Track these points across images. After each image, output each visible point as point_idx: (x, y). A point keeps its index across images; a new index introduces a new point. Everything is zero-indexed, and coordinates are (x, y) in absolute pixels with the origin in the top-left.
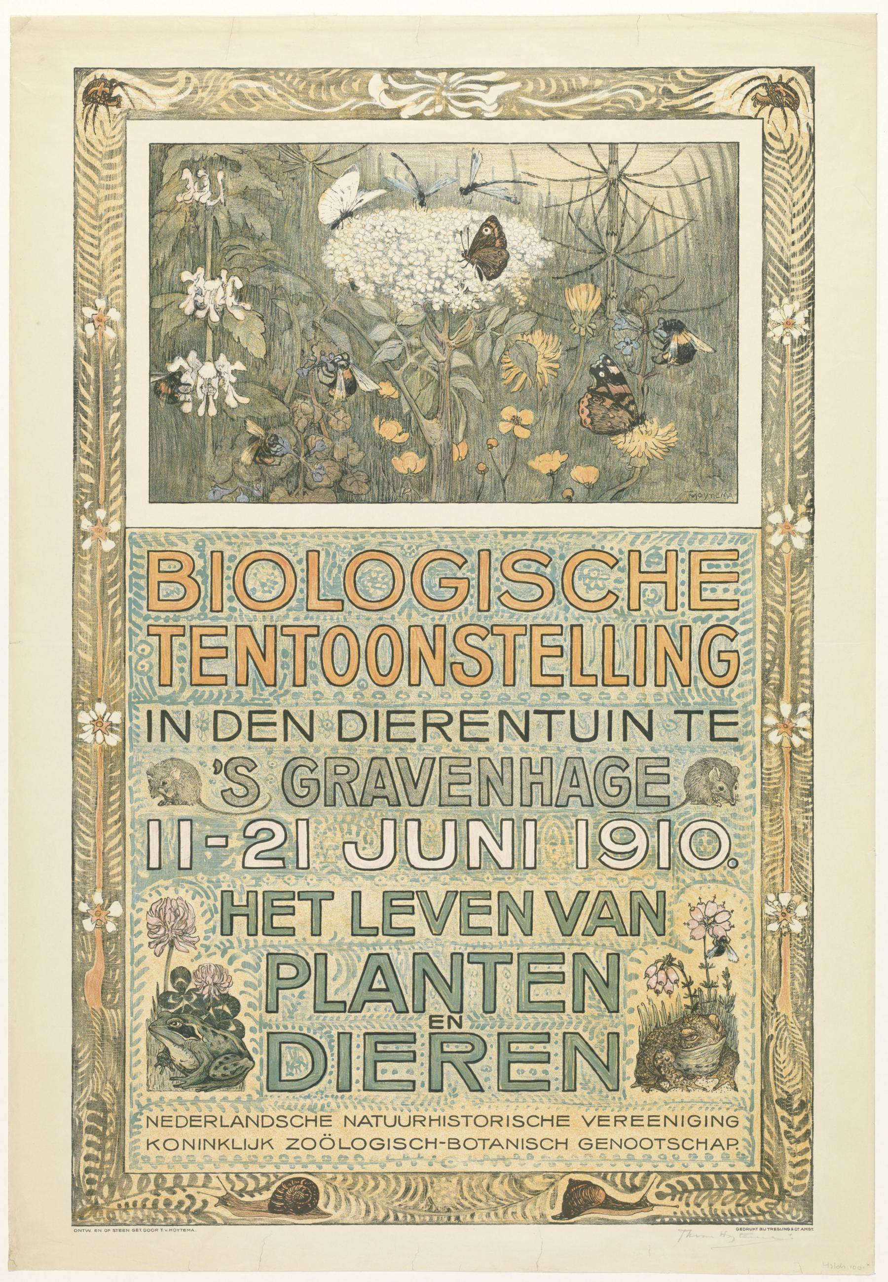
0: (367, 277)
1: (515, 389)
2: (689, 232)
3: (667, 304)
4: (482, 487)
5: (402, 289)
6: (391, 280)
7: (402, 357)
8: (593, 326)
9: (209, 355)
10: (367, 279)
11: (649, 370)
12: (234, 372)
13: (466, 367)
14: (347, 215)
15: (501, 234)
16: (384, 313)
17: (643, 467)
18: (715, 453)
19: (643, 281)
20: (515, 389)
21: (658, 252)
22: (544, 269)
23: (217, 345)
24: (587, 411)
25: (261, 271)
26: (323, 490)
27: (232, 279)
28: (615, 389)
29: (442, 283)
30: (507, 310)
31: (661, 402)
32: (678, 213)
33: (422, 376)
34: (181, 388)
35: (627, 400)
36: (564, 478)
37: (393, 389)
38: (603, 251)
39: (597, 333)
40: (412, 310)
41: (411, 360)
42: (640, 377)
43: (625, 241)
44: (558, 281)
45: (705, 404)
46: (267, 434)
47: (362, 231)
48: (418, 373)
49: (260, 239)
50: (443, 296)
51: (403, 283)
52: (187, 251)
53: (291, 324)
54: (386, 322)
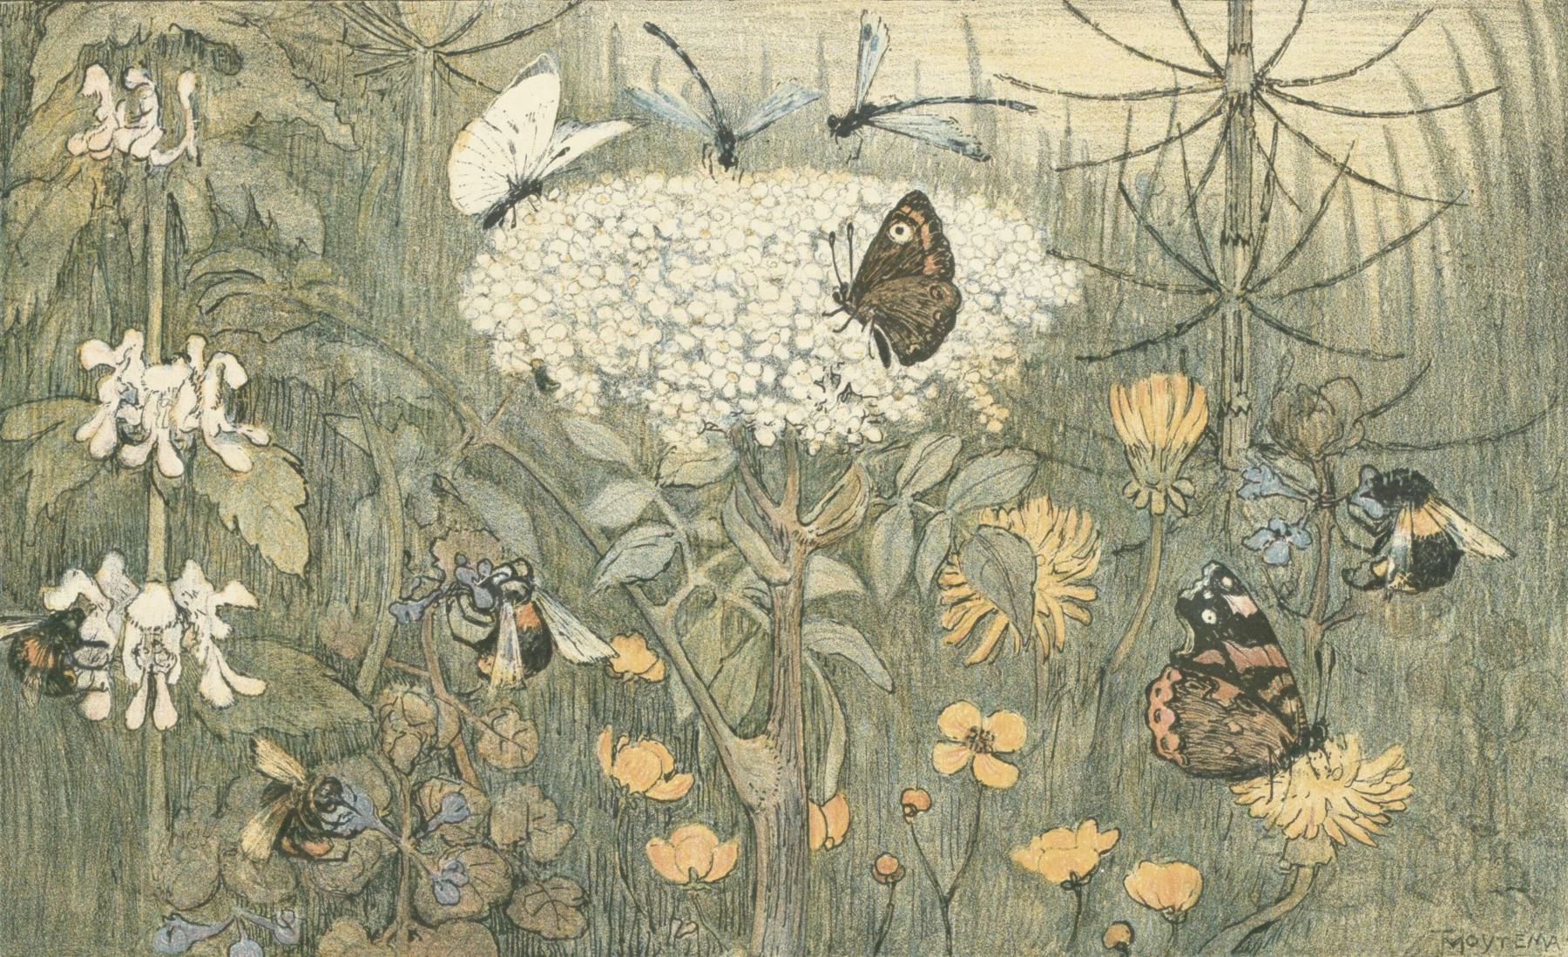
0: (579, 355)
1: (977, 655)
2: (1442, 235)
3: (1385, 429)
4: (889, 917)
5: (674, 387)
6: (644, 364)
7: (672, 571)
8: (1186, 487)
9: (157, 565)
10: (579, 362)
11: (1335, 605)
12: (223, 611)
13: (845, 597)
14: (526, 189)
15: (940, 242)
16: (625, 453)
17: (1318, 867)
18: (1511, 827)
19: (1320, 366)
20: (977, 655)
21: (1359, 289)
22: (1053, 336)
23: (178, 538)
24: (1168, 716)
25: (297, 338)
26: (462, 928)
27: (217, 361)
28: (1246, 656)
29: (782, 373)
30: (956, 443)
31: (1368, 690)
32: (1413, 185)
33: (726, 622)
34: (82, 655)
35: (1276, 686)
36: (1108, 896)
37: (649, 657)
38: (1213, 285)
39: (1196, 506)
40: (699, 445)
41: (697, 577)
42: (1310, 624)
43: (1269, 261)
44: (1093, 368)
45: (1485, 697)
46: (311, 777)
47: (567, 234)
48: (717, 614)
49: (294, 254)
50: (782, 408)
51: (676, 371)
52: (98, 286)
53: (376, 483)
54: (631, 476)
